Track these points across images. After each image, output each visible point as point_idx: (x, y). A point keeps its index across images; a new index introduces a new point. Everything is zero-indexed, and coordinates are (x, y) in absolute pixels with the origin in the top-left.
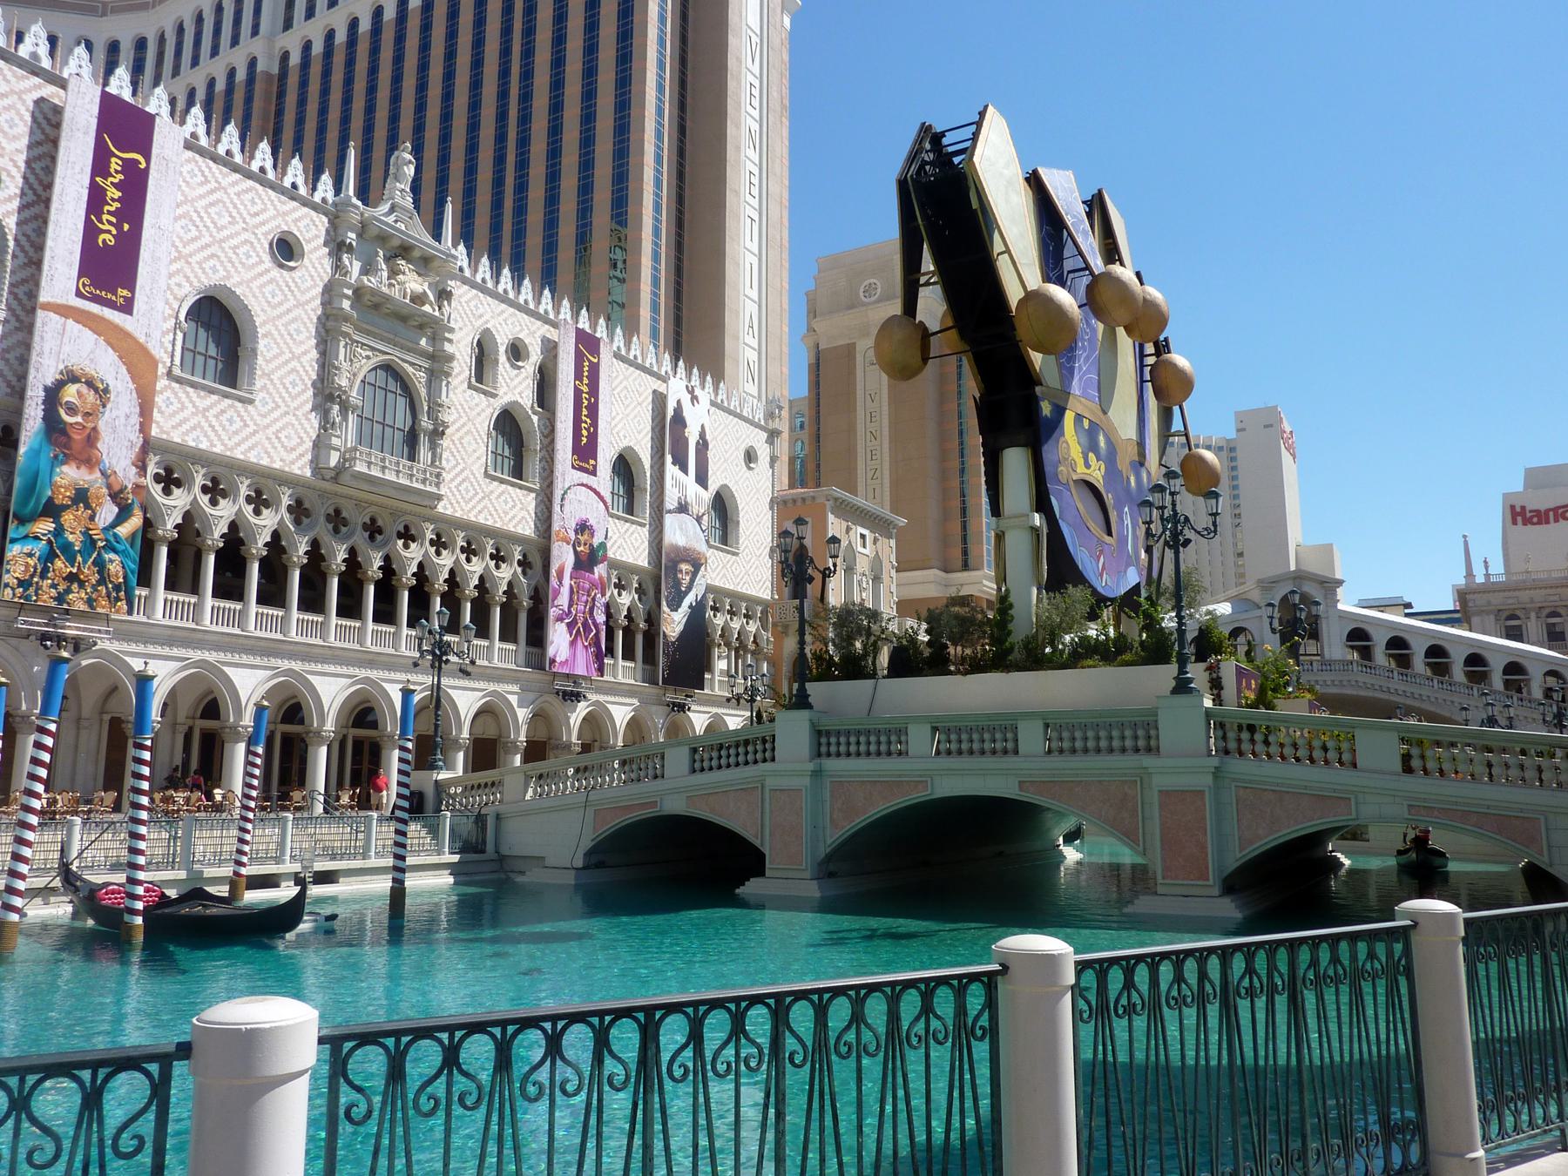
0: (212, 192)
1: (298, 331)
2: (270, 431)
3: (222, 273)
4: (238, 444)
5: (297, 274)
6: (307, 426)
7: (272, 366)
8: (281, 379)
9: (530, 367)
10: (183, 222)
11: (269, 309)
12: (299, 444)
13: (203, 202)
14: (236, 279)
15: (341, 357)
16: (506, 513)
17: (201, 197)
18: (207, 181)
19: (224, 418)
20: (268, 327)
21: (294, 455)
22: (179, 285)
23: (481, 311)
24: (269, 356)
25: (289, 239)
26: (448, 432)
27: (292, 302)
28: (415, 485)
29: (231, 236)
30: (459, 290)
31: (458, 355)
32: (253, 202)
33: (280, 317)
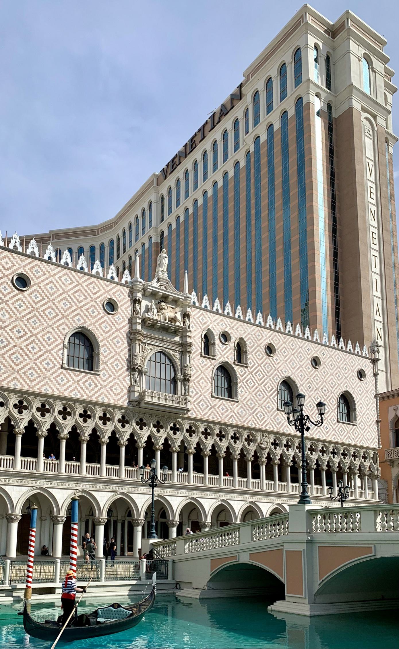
0: (76, 286)
1: (118, 342)
2: (107, 388)
3: (82, 321)
4: (94, 395)
5: (116, 317)
6: (125, 384)
7: (107, 359)
8: (111, 364)
9: (232, 344)
10: (64, 302)
11: (104, 334)
12: (121, 392)
13: (72, 291)
14: (89, 323)
15: (137, 351)
16: (223, 414)
17: (71, 289)
18: (73, 282)
19: (87, 384)
20: (105, 342)
21: (119, 397)
22: (64, 329)
23: (205, 321)
24: (105, 354)
25: (112, 302)
26: (191, 379)
27: (115, 329)
28: (175, 405)
29: (85, 305)
30: (193, 312)
31: (194, 343)
32: (94, 288)
33: (109, 337)
